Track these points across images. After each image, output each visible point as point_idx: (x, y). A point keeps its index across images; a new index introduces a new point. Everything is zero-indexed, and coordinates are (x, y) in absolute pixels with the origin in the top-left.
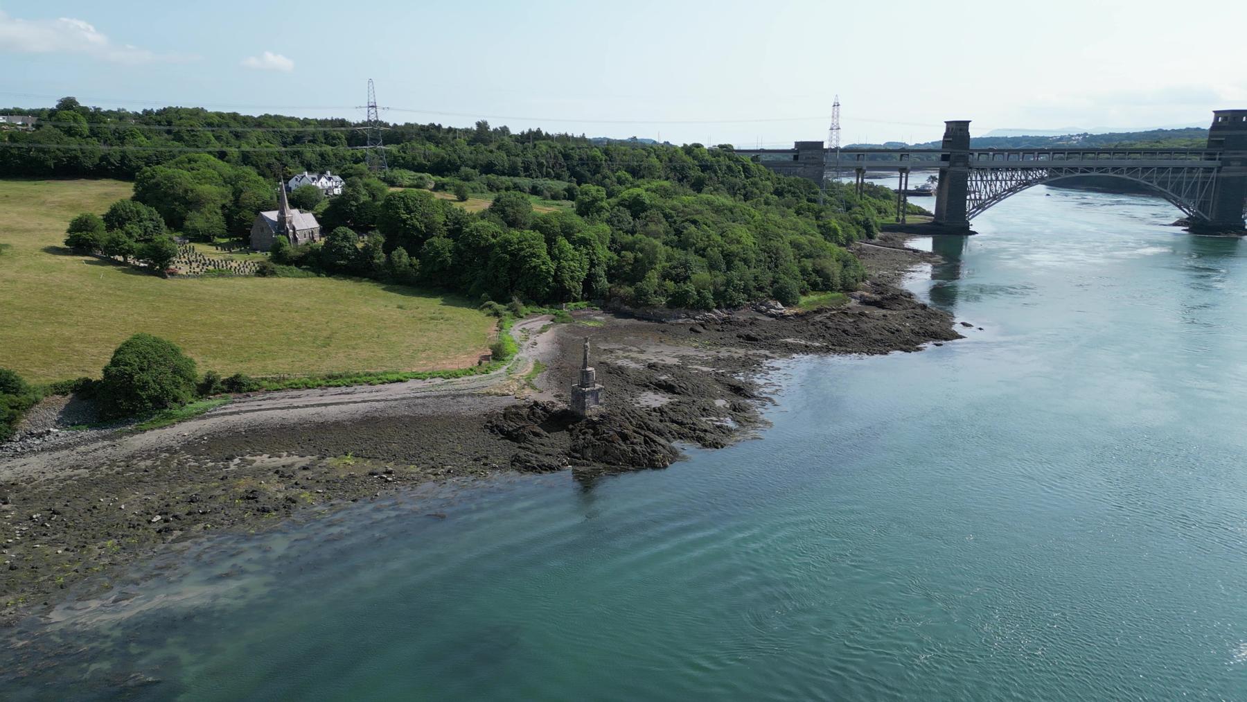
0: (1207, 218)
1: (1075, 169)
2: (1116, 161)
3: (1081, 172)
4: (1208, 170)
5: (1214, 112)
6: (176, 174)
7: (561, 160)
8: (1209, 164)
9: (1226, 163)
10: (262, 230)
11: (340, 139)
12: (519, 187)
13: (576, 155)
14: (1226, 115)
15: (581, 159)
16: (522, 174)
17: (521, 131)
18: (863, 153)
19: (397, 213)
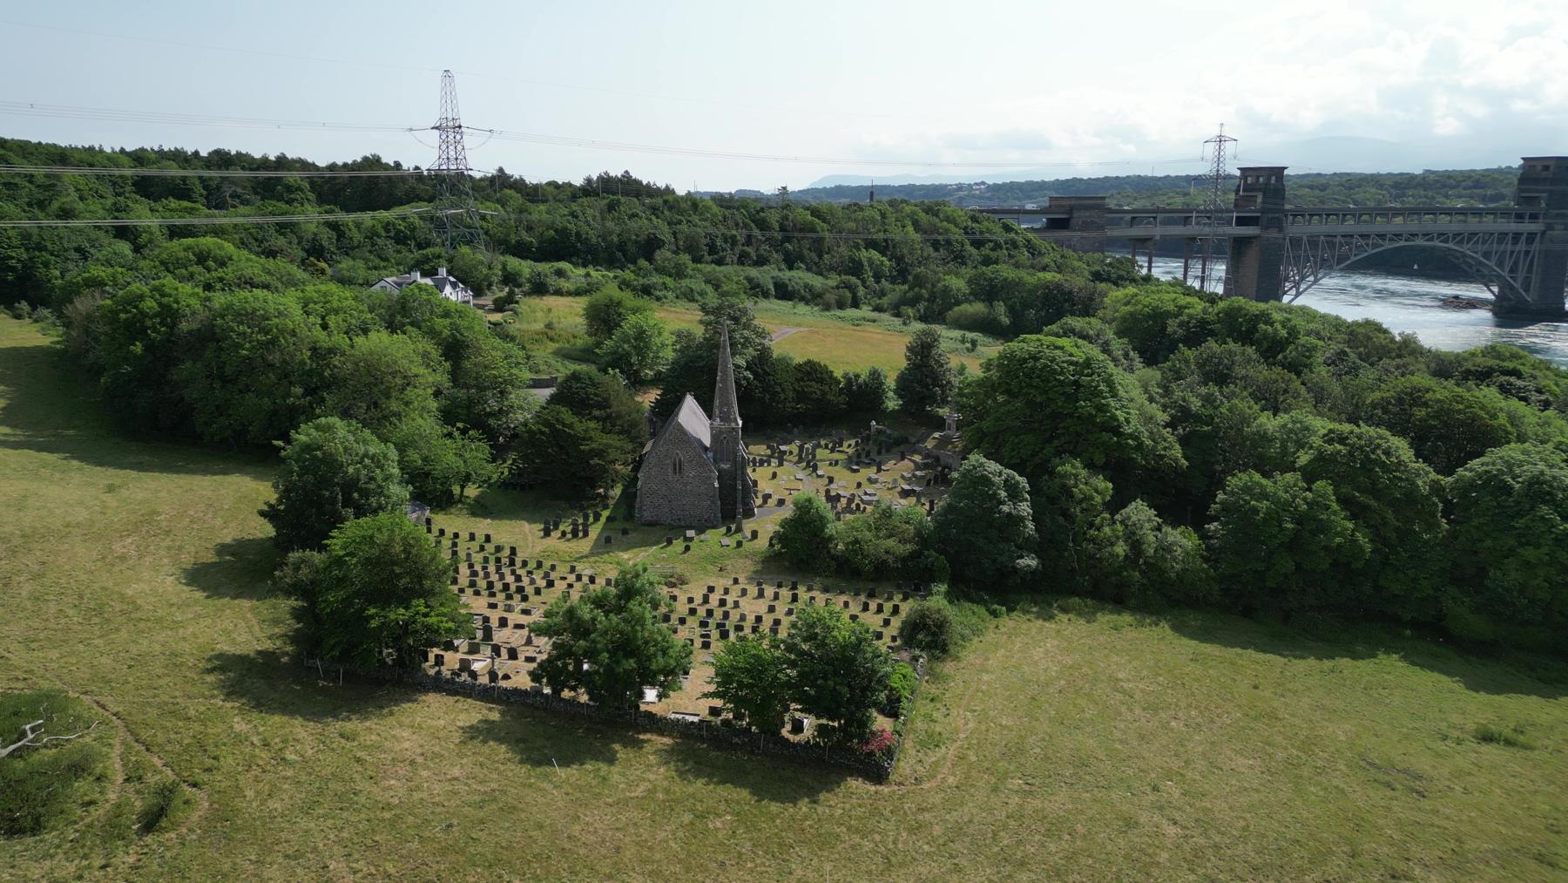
0: (1529, 299)
1: (1398, 235)
2: (1413, 225)
3: (1406, 240)
4: (1531, 237)
5: (1523, 159)
6: (271, 308)
7: (756, 232)
8: (1527, 227)
9: (1550, 227)
10: (678, 468)
11: (302, 190)
12: (758, 286)
13: (773, 218)
14: (1546, 163)
15: (783, 229)
16: (709, 258)
17: (585, 175)
18: (1154, 215)
19: (1102, 409)
